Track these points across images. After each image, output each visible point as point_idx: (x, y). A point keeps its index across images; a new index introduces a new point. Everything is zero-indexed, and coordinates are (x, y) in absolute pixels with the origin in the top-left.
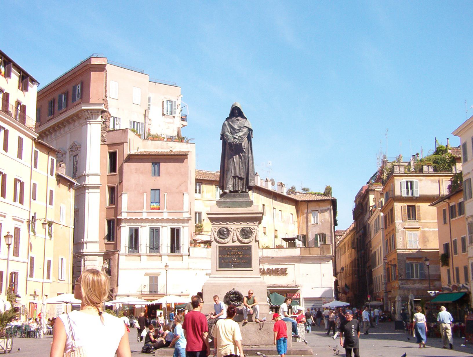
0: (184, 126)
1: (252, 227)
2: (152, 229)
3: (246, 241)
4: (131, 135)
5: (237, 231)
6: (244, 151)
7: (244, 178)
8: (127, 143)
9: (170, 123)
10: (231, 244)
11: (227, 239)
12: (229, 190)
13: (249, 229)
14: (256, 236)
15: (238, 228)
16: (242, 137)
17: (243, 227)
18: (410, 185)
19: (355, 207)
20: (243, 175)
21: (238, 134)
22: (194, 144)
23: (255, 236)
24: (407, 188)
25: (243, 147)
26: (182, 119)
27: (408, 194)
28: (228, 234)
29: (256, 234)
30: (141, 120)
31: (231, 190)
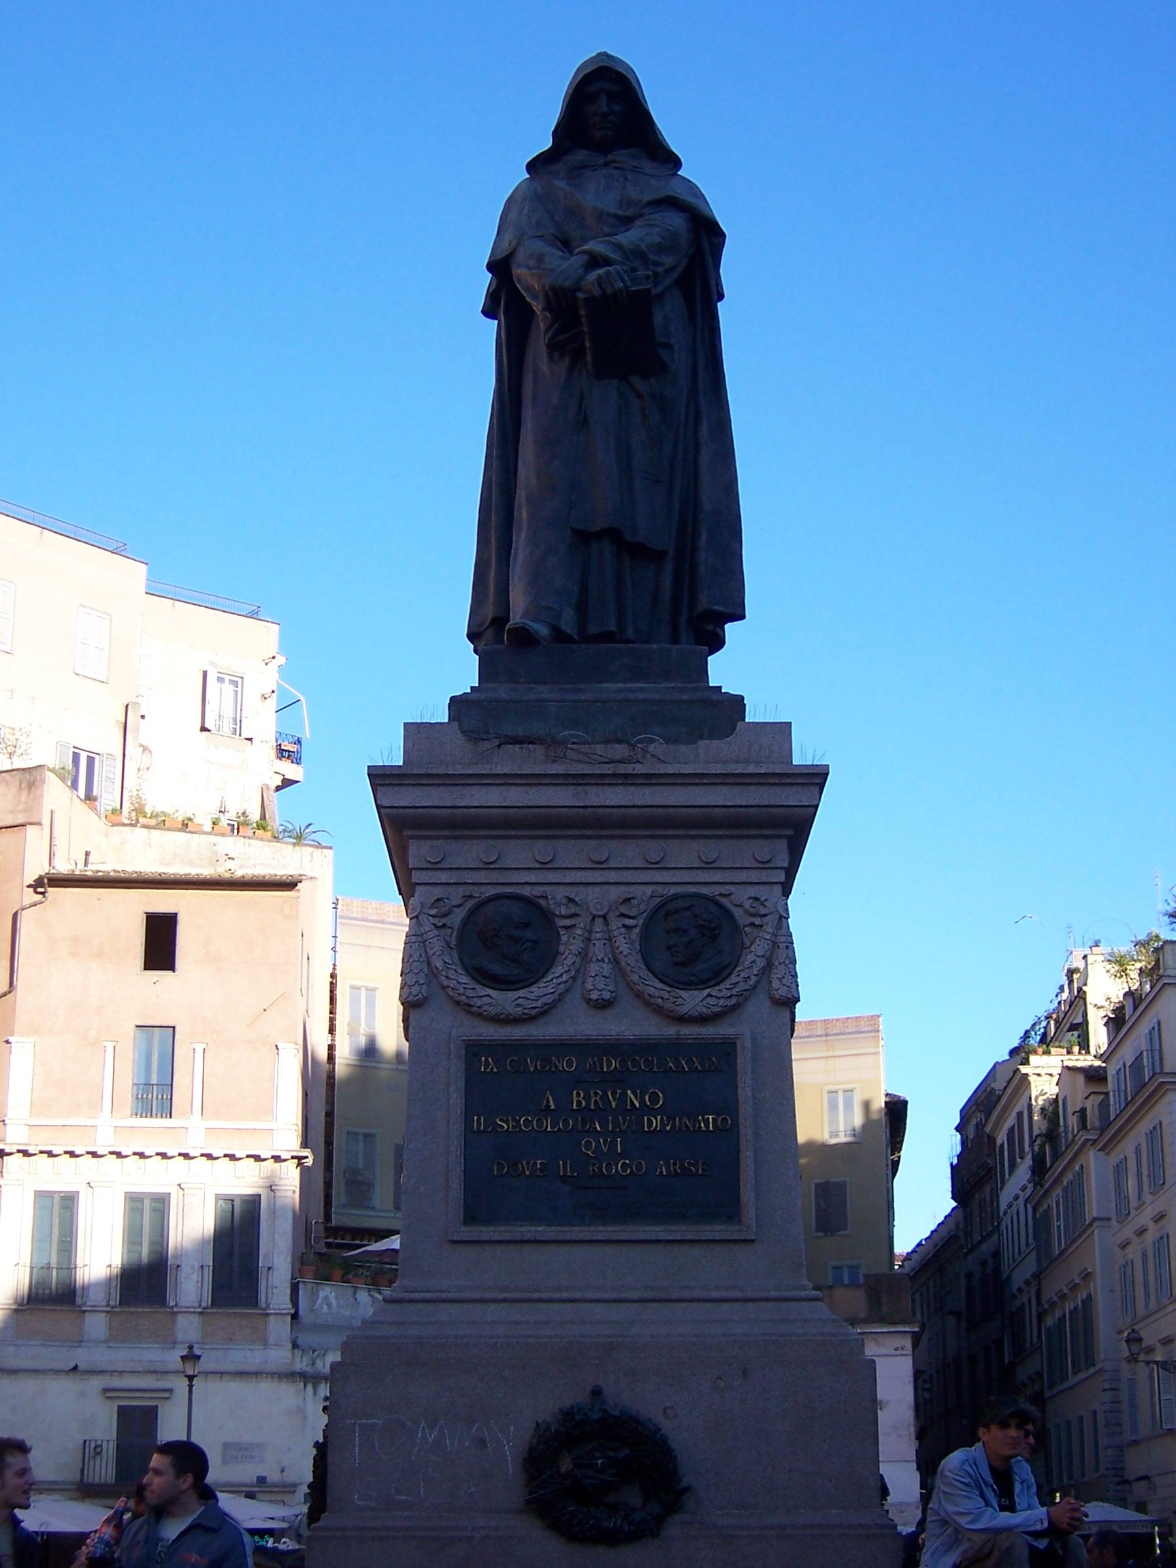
0: (287, 783)
1: (743, 895)
2: (134, 1202)
3: (692, 1001)
4: (55, 794)
5: (615, 924)
7: (659, 556)
8: (39, 824)
11: (536, 990)
14: (769, 965)
15: (627, 900)
19: (959, 1149)
21: (622, 238)
22: (331, 848)
23: (761, 963)
26: (281, 753)
28: (552, 957)
30: (105, 742)
31: (564, 627)
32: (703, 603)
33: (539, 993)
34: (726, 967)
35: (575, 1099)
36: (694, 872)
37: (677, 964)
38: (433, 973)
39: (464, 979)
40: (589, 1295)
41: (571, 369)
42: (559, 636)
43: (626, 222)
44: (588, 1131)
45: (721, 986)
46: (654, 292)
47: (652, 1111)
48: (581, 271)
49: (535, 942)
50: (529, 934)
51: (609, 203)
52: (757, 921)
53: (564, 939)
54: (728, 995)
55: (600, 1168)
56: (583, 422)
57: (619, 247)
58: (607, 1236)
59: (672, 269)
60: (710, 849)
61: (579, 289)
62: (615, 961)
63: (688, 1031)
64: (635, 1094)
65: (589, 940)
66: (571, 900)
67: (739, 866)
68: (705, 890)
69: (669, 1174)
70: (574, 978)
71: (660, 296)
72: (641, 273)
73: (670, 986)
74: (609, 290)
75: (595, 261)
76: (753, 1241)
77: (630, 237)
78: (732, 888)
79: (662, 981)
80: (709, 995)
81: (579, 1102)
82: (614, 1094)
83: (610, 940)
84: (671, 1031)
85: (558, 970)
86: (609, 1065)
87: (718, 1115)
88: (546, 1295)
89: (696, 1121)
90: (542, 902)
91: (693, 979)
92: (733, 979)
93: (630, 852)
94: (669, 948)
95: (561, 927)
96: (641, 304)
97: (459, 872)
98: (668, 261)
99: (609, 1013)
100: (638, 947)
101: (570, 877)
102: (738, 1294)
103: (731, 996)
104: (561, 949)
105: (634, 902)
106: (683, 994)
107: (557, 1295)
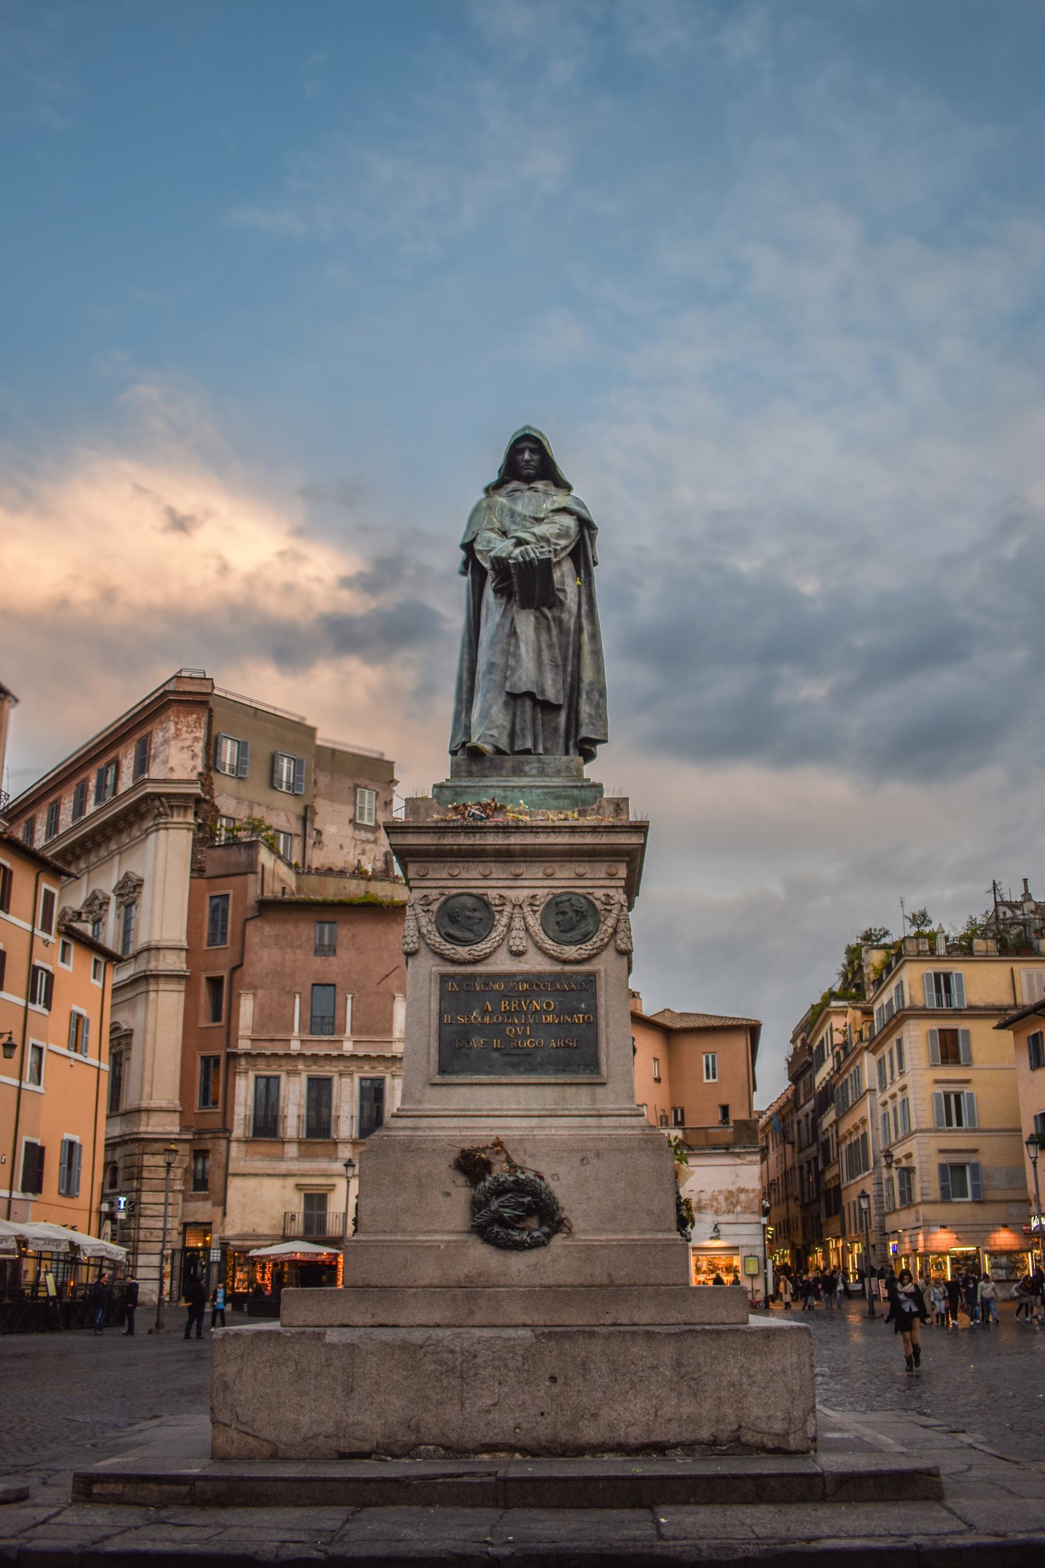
3: (571, 952)
4: (265, 857)
5: (527, 909)
6: (561, 602)
7: (558, 708)
8: (256, 873)
9: (368, 842)
10: (502, 963)
11: (481, 946)
12: (496, 747)
13: (583, 901)
15: (534, 897)
16: (553, 540)
17: (555, 891)
18: (943, 983)
20: (553, 692)
23: (610, 930)
24: (938, 990)
25: (557, 586)
27: (940, 1004)
28: (491, 927)
29: (618, 920)
30: (295, 827)
31: (501, 747)
32: (585, 732)
33: (483, 947)
34: (590, 933)
35: (503, 1005)
36: (571, 881)
37: (562, 931)
38: (421, 936)
39: (439, 939)
40: (510, 1113)
41: (508, 602)
42: (499, 751)
43: (539, 520)
44: (511, 1023)
45: (587, 944)
46: (555, 560)
47: (547, 1012)
48: (511, 548)
49: (480, 919)
50: (477, 914)
51: (528, 511)
52: (609, 907)
53: (497, 917)
54: (591, 947)
55: (517, 1044)
56: (513, 633)
57: (534, 534)
58: (522, 1081)
59: (566, 547)
60: (581, 869)
61: (510, 558)
62: (527, 930)
63: (568, 968)
64: (538, 1003)
65: (512, 918)
66: (501, 896)
67: (597, 877)
68: (579, 891)
69: (557, 1047)
70: (503, 939)
71: (559, 563)
72: (546, 549)
73: (558, 943)
74: (528, 559)
75: (520, 542)
76: (604, 1084)
77: (540, 530)
78: (594, 890)
79: (553, 941)
80: (580, 948)
81: (505, 1007)
82: (525, 1003)
83: (524, 918)
84: (558, 968)
85: (494, 935)
86: (523, 987)
87: (585, 1014)
88: (485, 1113)
89: (572, 1018)
90: (485, 897)
91: (572, 940)
92: (595, 939)
93: (535, 871)
94: (558, 923)
95: (496, 911)
96: (547, 566)
97: (438, 881)
98: (563, 543)
99: (522, 959)
100: (539, 922)
101: (501, 883)
102: (595, 1113)
103: (593, 949)
104: (496, 923)
105: (538, 897)
106: (564, 947)
107: (492, 1113)
